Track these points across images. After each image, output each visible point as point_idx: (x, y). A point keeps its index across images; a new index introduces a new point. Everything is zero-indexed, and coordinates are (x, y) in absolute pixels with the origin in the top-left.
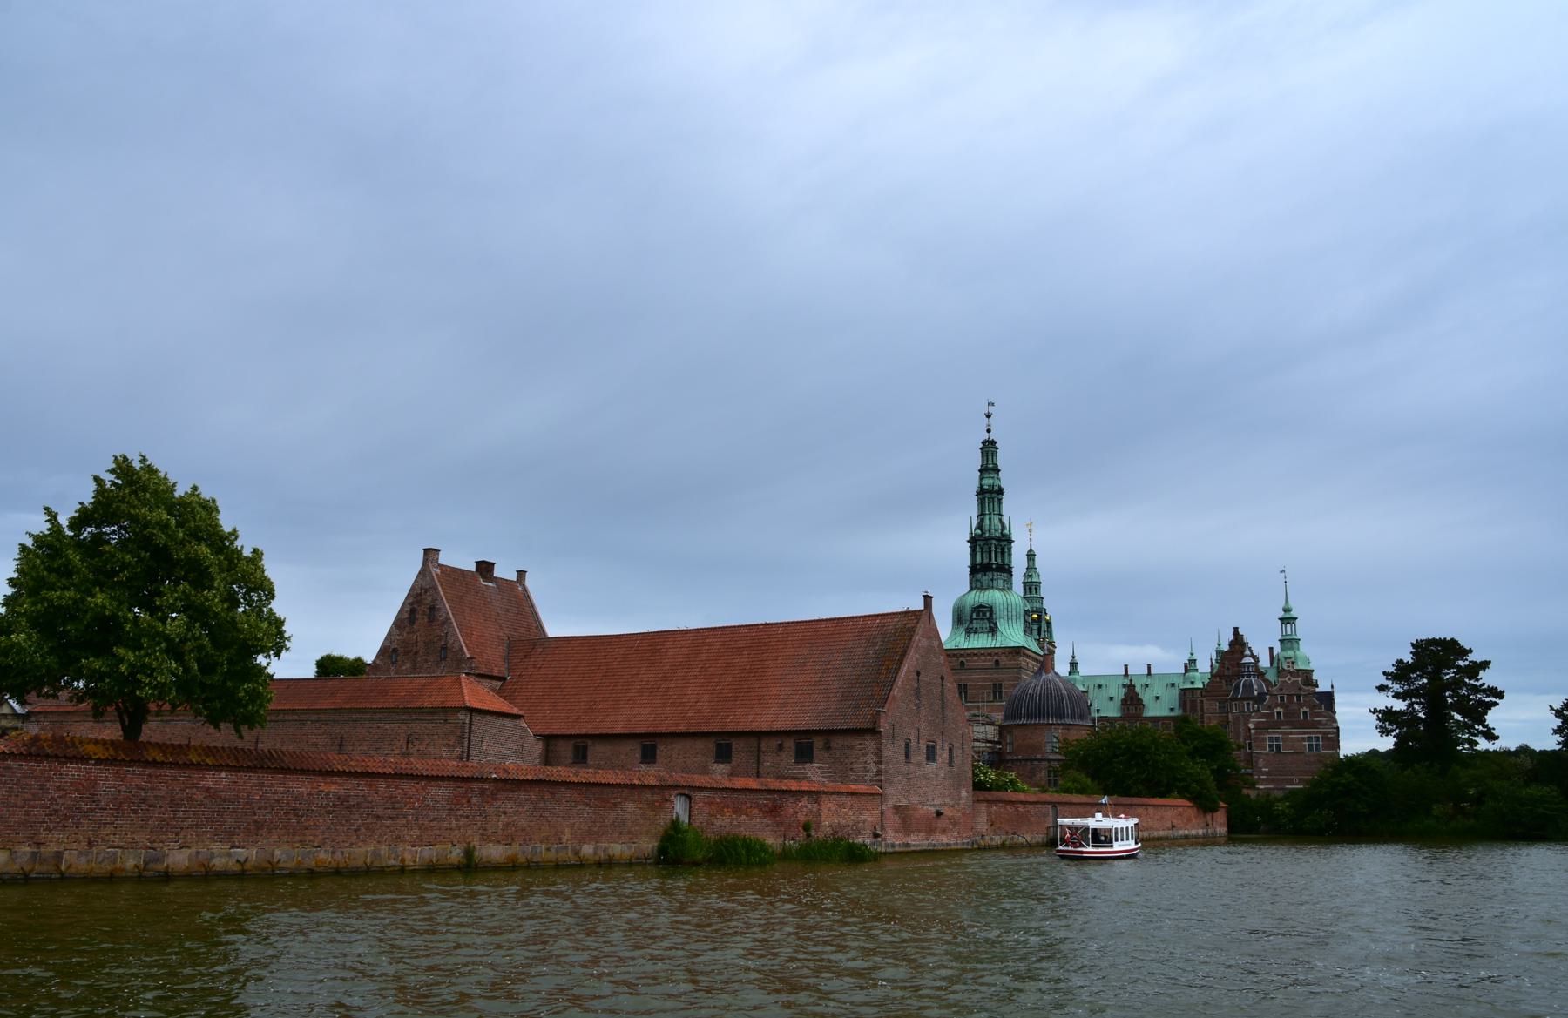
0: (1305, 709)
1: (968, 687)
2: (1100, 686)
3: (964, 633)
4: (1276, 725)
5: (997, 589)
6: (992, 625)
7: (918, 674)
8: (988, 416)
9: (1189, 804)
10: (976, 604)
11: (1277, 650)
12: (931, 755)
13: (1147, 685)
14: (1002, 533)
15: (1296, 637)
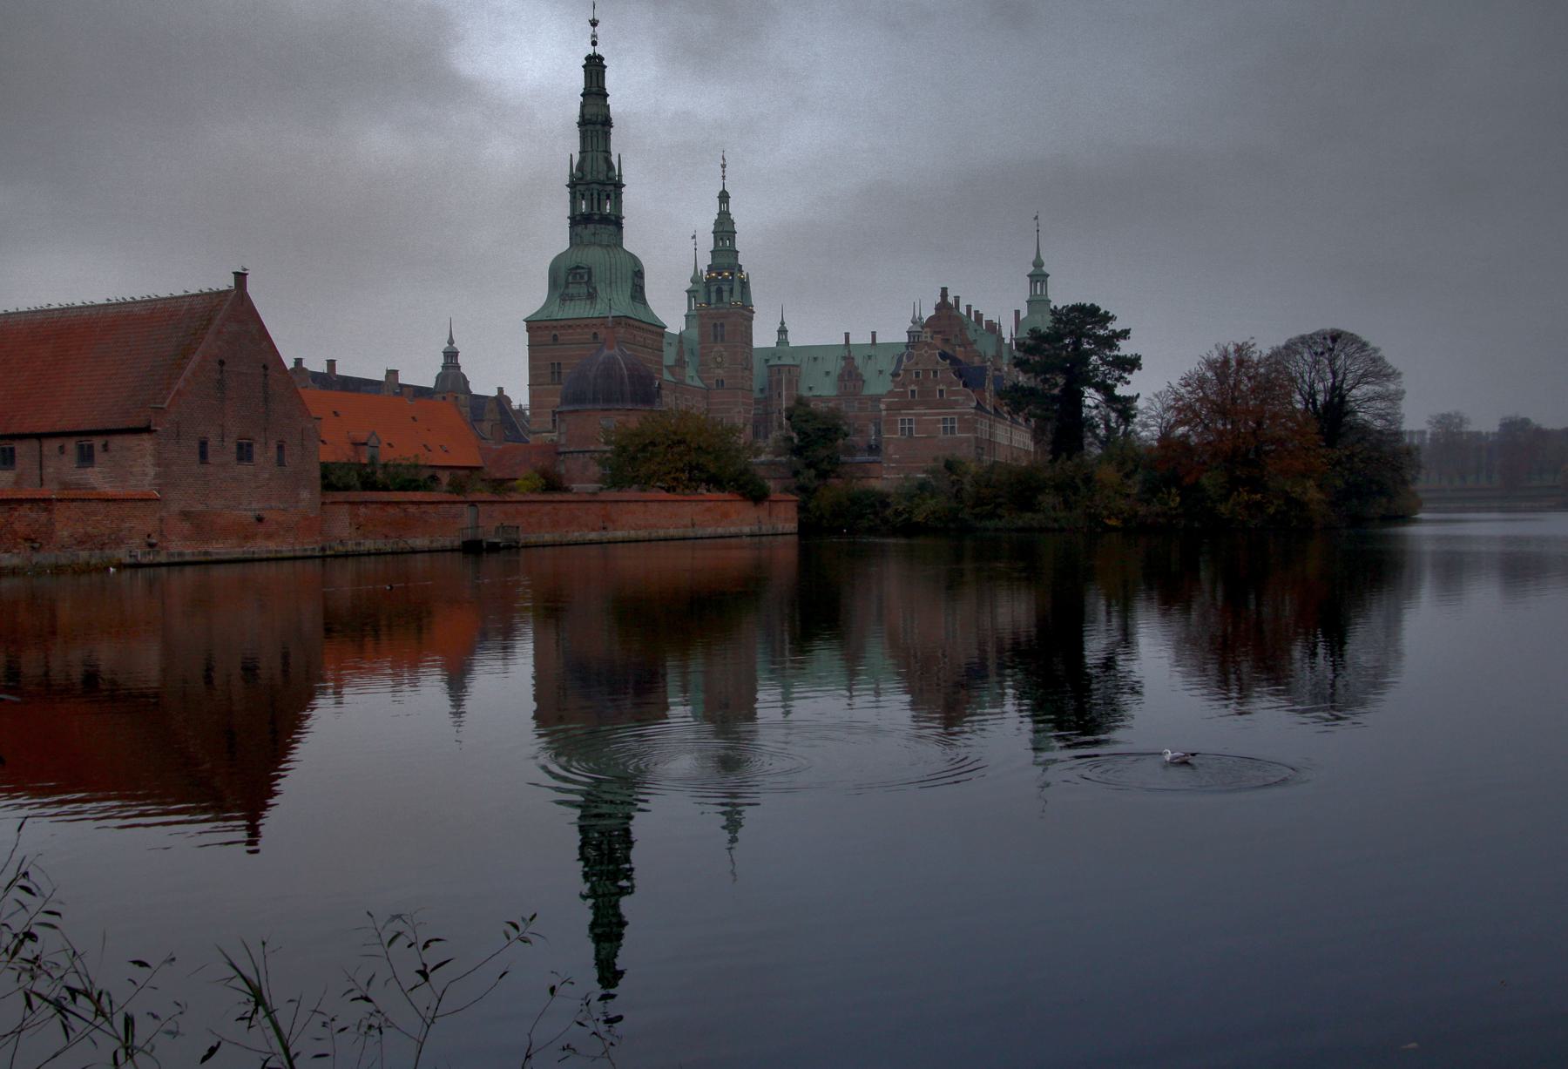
0: (941, 387)
1: (562, 366)
2: (815, 359)
3: (558, 300)
4: (909, 406)
5: (600, 245)
6: (591, 290)
7: (222, 363)
8: (594, 23)
9: (739, 498)
10: (573, 265)
11: (1024, 313)
12: (244, 452)
13: (870, 357)
14: (607, 175)
15: (1045, 298)
